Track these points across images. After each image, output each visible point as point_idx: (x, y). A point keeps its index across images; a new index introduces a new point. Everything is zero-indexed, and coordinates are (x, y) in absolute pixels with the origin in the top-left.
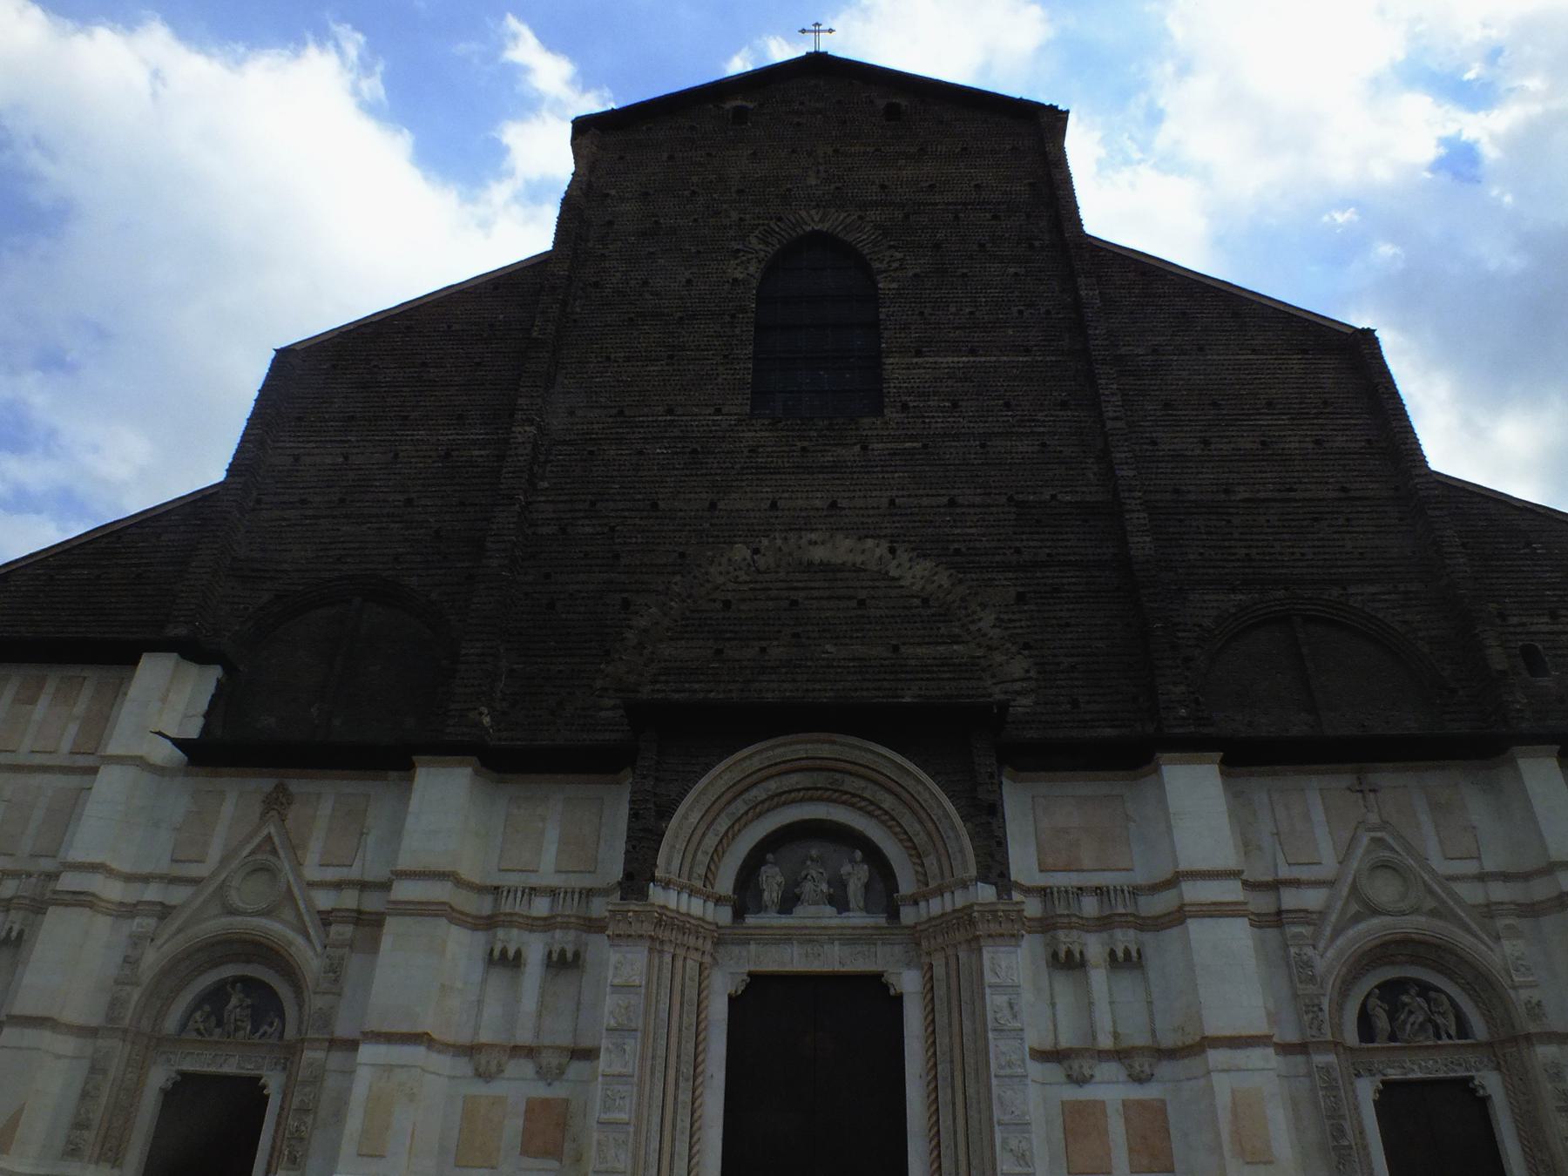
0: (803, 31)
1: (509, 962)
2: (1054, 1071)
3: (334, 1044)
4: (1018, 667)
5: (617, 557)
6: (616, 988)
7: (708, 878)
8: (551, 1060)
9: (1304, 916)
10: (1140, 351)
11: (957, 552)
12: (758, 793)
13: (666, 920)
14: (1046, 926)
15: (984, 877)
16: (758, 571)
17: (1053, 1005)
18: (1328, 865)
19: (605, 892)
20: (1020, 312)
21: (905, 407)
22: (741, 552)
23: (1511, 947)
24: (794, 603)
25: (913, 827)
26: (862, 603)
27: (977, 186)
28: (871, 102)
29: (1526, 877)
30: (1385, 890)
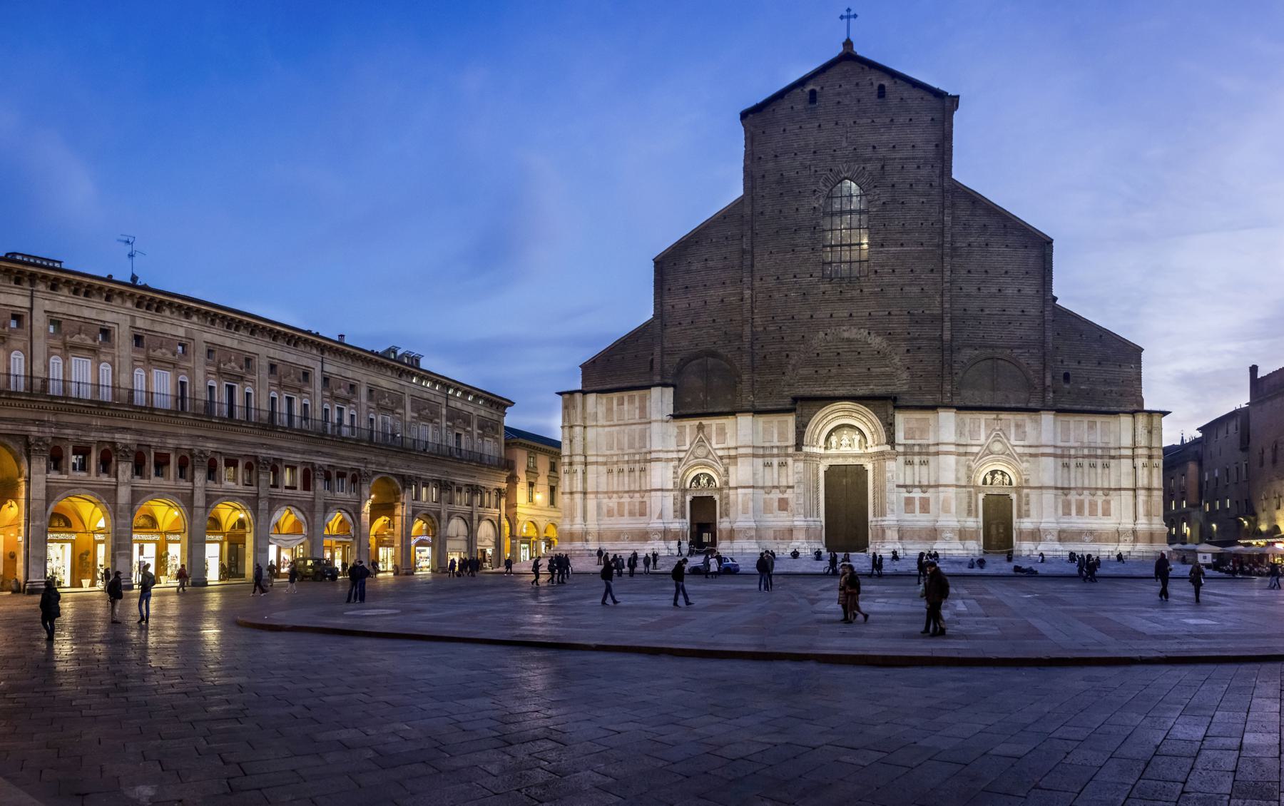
0: (842, 17)
1: (771, 465)
2: (904, 490)
3: (730, 488)
4: (905, 375)
5: (783, 338)
6: (797, 473)
7: (817, 442)
8: (782, 489)
9: (972, 454)
10: (964, 245)
11: (890, 334)
12: (830, 417)
13: (807, 455)
14: (905, 454)
15: (887, 443)
16: (827, 342)
17: (905, 474)
18: (982, 439)
19: (792, 446)
20: (922, 224)
21: (876, 272)
22: (821, 334)
23: (1025, 465)
24: (839, 354)
25: (871, 427)
26: (859, 353)
27: (913, 146)
28: (872, 84)
29: (1037, 446)
30: (997, 447)
